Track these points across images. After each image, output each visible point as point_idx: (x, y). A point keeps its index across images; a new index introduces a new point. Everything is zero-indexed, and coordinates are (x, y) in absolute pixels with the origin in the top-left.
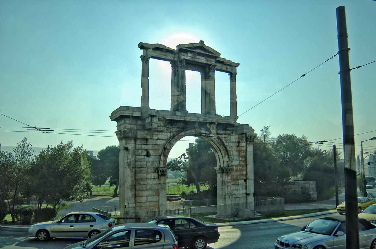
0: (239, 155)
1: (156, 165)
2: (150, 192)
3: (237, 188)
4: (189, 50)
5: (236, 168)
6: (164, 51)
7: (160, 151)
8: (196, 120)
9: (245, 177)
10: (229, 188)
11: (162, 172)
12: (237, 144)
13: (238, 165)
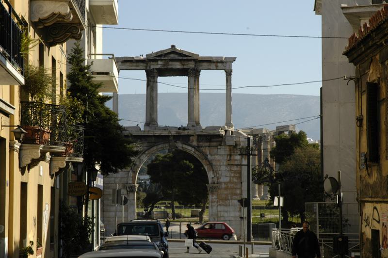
0: (231, 170)
1: (125, 181)
3: (226, 209)
4: (158, 58)
9: (238, 197)
10: (215, 208)
12: (227, 157)
13: (228, 182)
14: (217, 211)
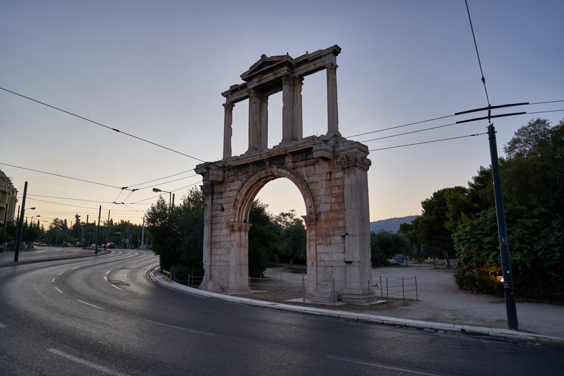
0: (332, 194)
2: (224, 251)
5: (326, 216)
6: (240, 91)
7: (232, 204)
8: (259, 158)
9: (342, 231)
11: (231, 227)
13: (328, 211)
14: (316, 253)
